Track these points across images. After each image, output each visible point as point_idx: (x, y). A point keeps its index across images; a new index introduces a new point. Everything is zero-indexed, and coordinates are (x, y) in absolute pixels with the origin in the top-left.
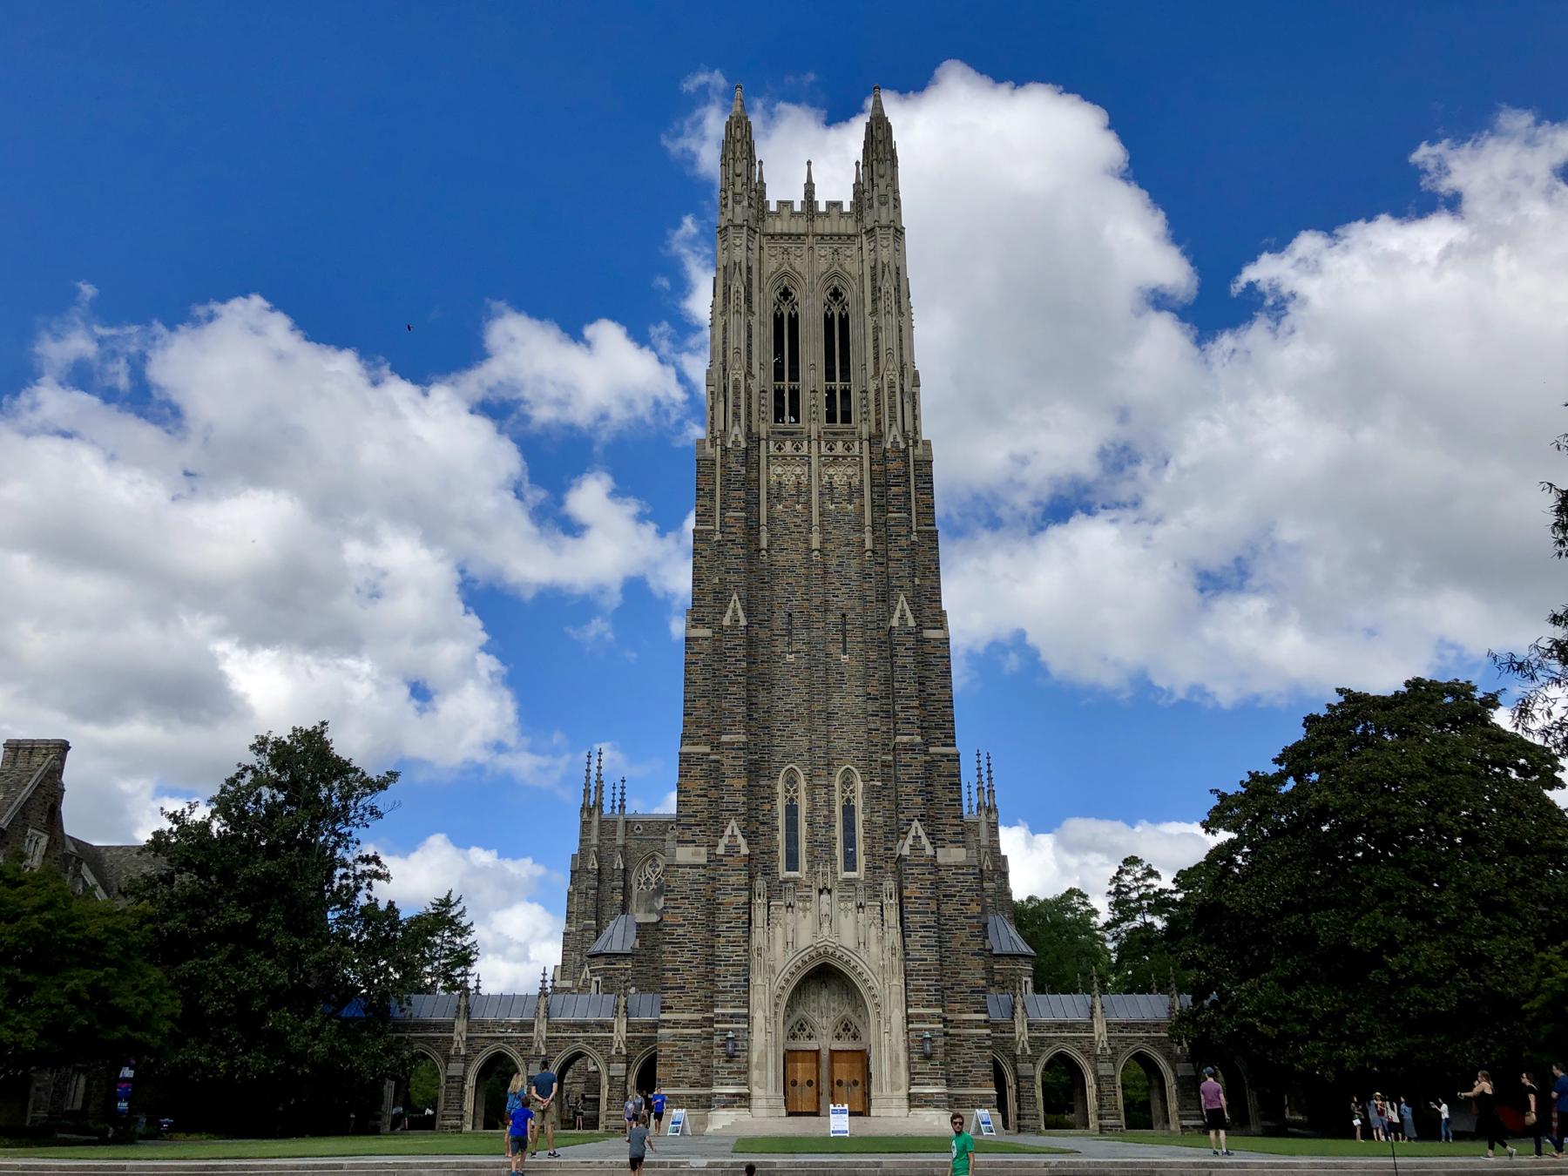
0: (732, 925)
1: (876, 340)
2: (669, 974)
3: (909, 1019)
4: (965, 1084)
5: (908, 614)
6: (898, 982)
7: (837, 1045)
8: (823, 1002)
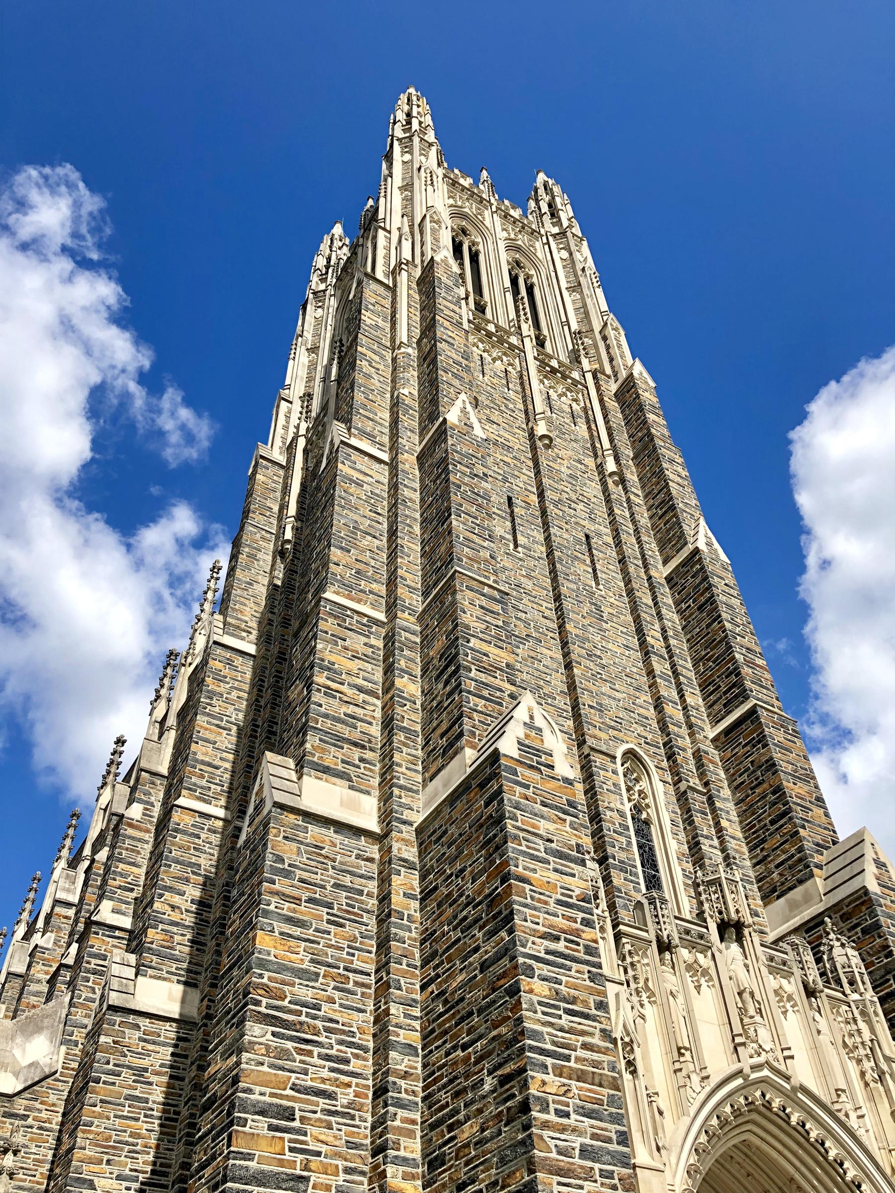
0: (561, 946)
2: (258, 1125)
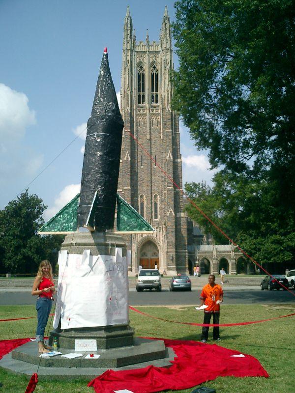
1: (164, 81)
3: (167, 252)
4: (181, 266)
5: (171, 156)
6: (166, 244)
7: (152, 258)
8: (149, 248)
